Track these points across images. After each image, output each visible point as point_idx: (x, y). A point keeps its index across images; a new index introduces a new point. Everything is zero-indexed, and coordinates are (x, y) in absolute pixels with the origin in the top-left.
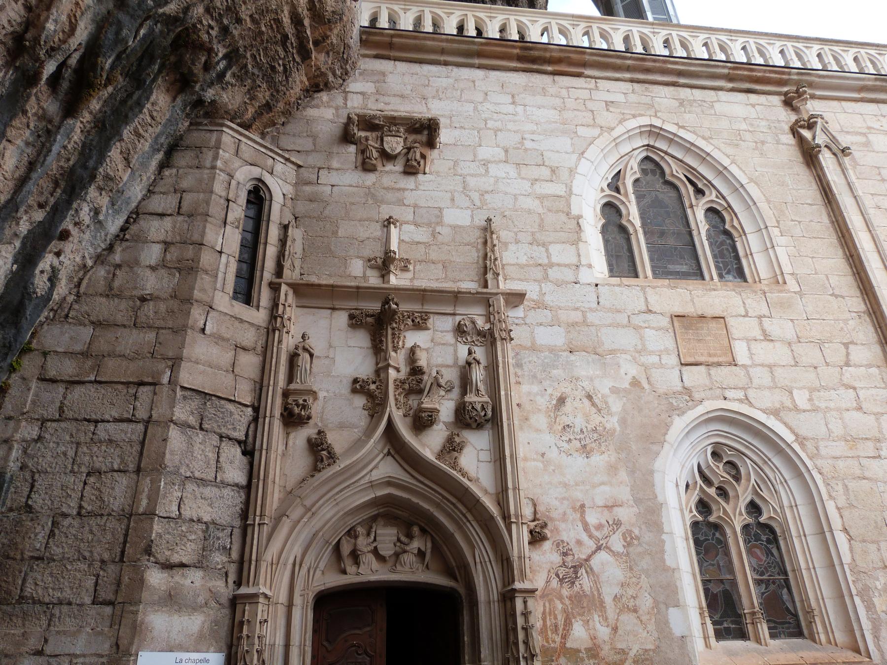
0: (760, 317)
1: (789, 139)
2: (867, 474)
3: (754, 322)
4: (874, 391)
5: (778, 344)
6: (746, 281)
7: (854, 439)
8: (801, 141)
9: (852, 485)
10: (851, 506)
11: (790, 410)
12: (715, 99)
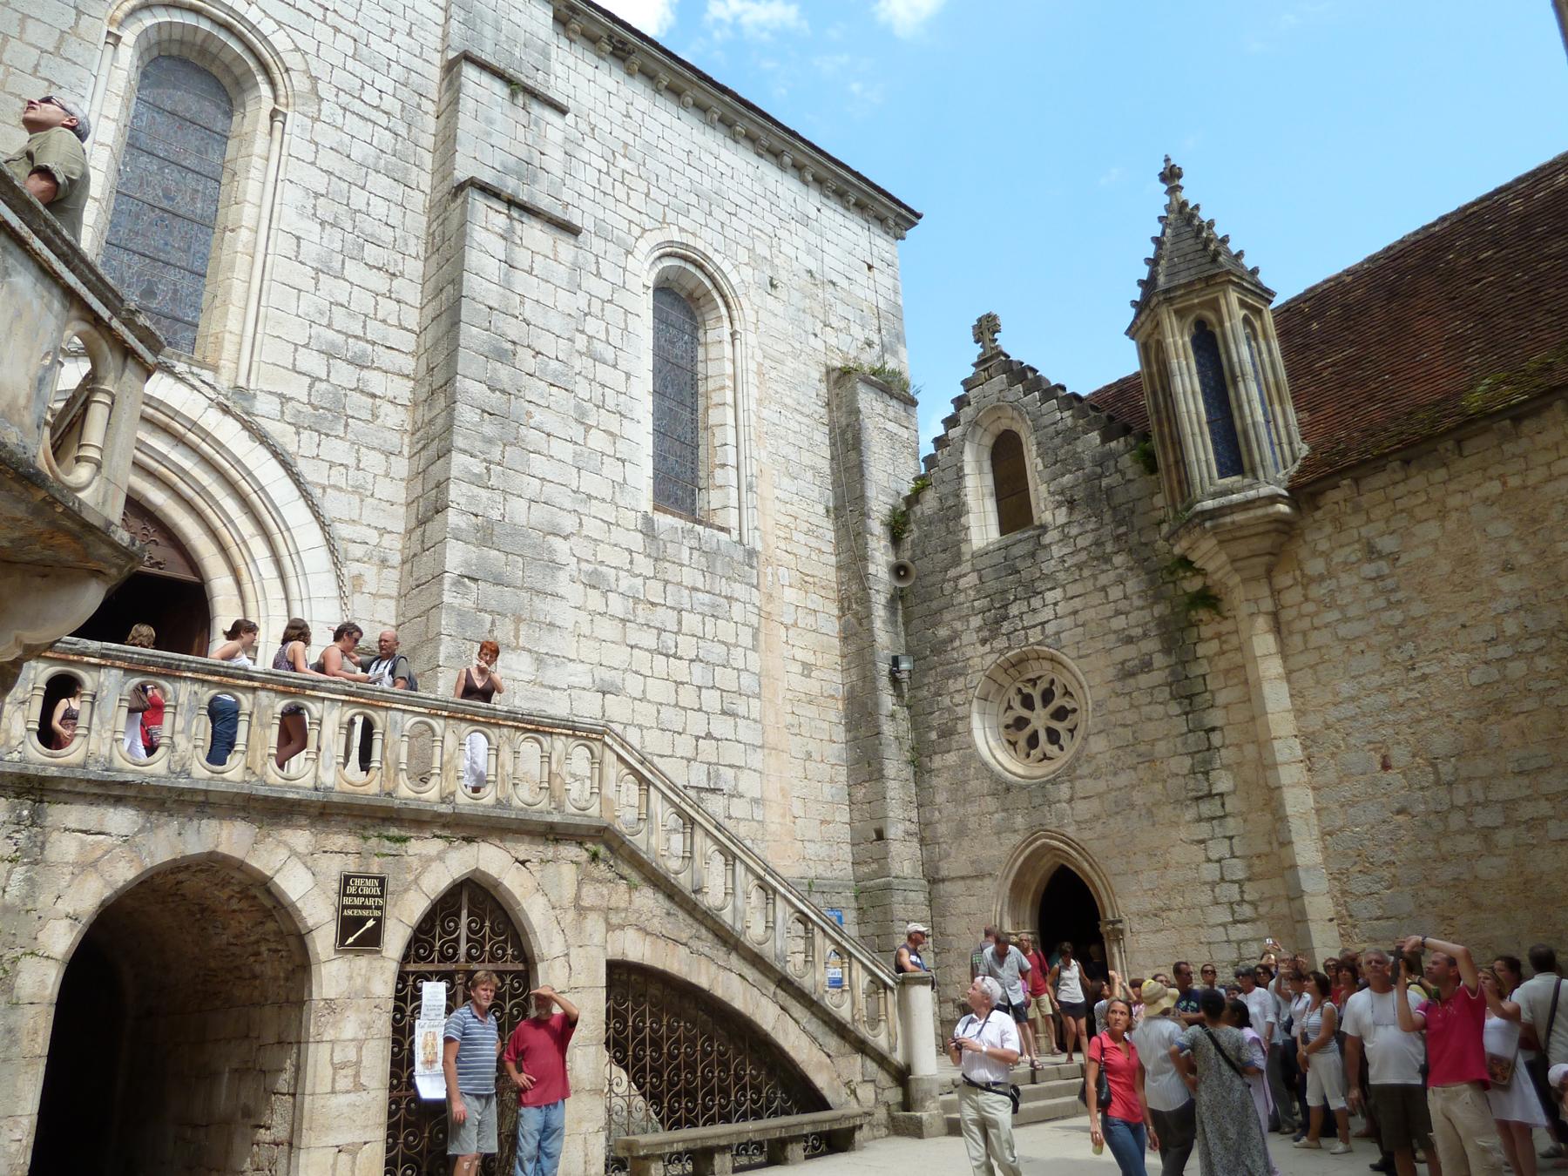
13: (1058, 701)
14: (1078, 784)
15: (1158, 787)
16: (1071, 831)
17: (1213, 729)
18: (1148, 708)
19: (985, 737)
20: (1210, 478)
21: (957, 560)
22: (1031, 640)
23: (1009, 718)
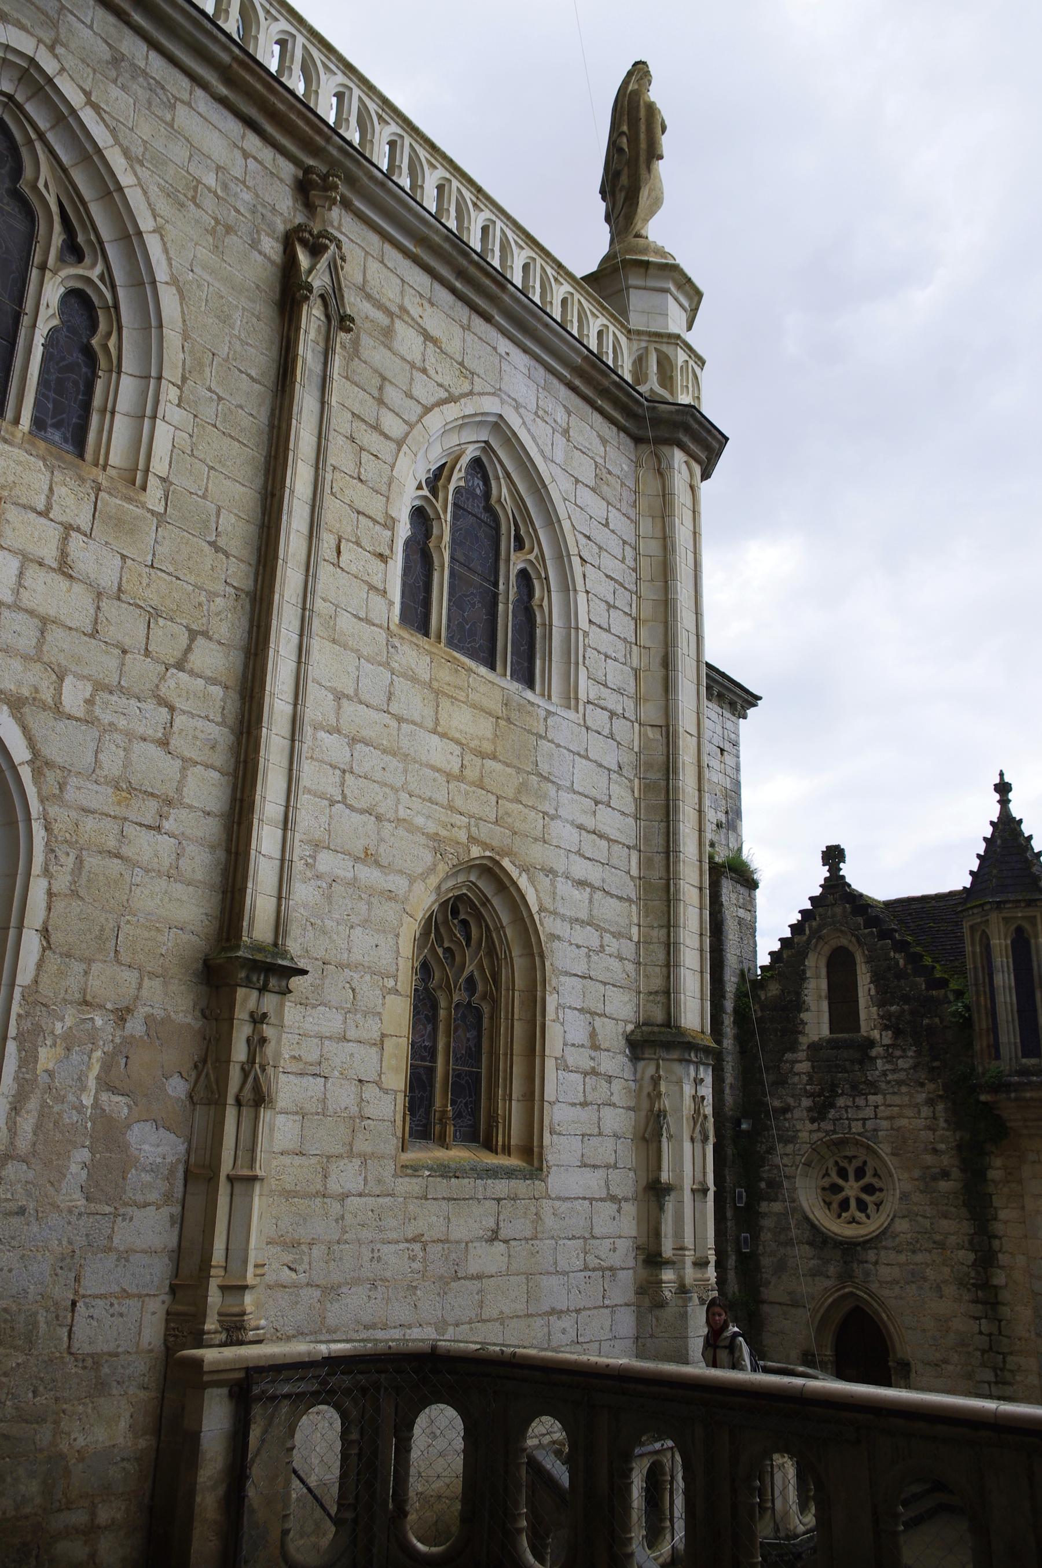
0: (69, 528)
1: (271, 247)
2: (125, 851)
3: (52, 533)
4: (200, 723)
5: (78, 588)
6: (81, 456)
7: (131, 789)
8: (290, 264)
9: (92, 862)
10: (75, 894)
11: (45, 707)
12: (185, 96)
13: (868, 1179)
14: (883, 1253)
15: (946, 1270)
16: (874, 1287)
17: (996, 1237)
18: (945, 1208)
19: (808, 1197)
20: (1016, 1057)
21: (793, 1047)
22: (854, 1130)
23: (826, 1182)
